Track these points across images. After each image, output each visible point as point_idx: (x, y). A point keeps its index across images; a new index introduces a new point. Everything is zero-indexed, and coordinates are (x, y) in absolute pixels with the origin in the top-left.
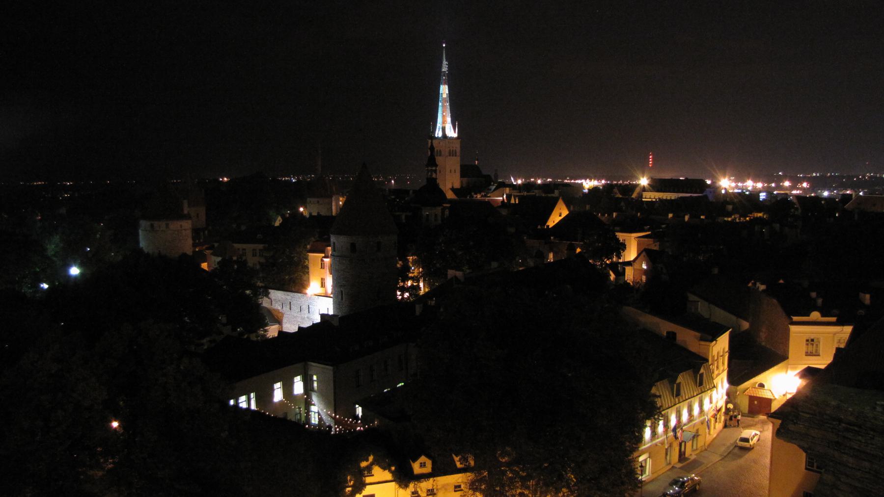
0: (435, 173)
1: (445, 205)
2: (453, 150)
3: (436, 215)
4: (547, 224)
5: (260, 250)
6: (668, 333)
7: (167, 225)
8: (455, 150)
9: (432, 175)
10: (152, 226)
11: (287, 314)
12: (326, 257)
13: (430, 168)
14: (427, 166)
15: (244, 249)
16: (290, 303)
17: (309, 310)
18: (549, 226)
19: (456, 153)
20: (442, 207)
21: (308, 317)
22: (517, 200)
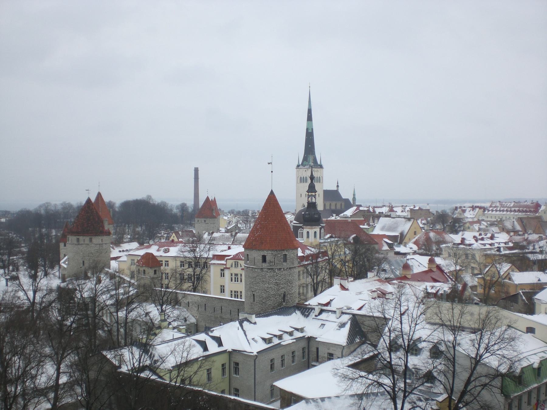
0: (315, 197)
1: (322, 225)
3: (315, 232)
4: (404, 241)
5: (166, 261)
6: (527, 328)
7: (91, 240)
8: (319, 177)
9: (312, 199)
10: (78, 240)
11: (202, 314)
12: (226, 268)
13: (310, 194)
14: (308, 192)
16: (205, 304)
20: (321, 227)
21: (221, 317)
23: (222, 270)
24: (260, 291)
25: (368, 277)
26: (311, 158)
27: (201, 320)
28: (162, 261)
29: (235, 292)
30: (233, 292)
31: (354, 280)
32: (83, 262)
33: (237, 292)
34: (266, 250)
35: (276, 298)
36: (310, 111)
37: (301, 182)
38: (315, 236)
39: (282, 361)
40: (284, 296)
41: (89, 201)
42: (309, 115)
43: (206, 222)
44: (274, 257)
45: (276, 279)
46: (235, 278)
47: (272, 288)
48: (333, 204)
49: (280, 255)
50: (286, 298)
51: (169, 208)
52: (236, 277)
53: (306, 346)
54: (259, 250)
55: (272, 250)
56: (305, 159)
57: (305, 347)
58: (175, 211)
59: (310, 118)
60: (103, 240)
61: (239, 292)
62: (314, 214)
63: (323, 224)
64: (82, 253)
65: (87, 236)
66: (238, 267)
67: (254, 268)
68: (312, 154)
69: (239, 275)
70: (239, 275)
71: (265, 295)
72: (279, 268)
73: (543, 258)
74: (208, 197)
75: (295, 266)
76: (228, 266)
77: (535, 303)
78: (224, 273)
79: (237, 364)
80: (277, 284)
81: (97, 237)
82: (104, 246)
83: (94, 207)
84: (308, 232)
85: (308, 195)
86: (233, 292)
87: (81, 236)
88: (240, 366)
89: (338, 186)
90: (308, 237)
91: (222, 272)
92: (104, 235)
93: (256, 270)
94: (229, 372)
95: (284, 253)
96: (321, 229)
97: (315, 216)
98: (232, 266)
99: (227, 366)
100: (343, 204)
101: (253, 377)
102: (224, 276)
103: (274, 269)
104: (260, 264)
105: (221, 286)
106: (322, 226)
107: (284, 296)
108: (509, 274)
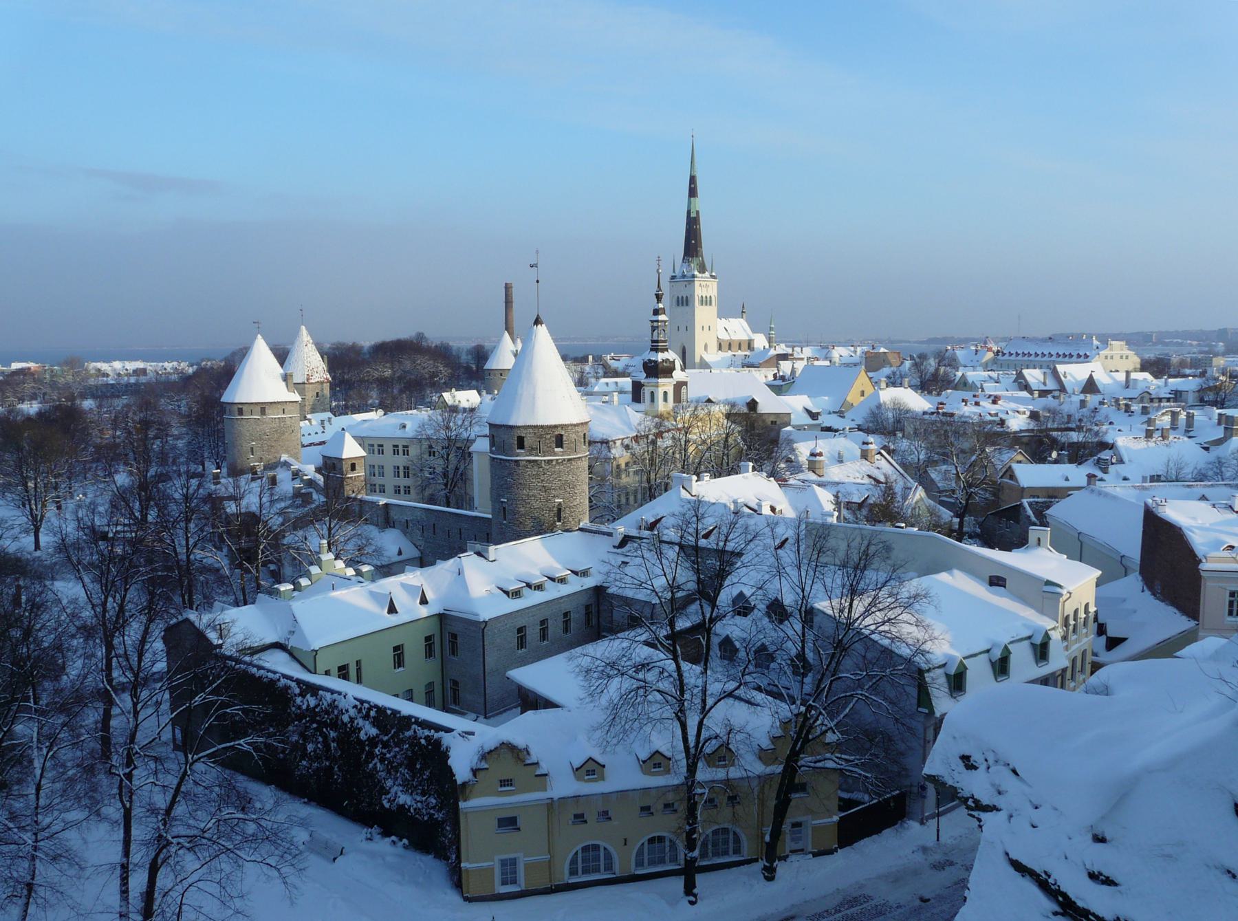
2: (706, 297)
3: (665, 393)
5: (404, 446)
6: (990, 577)
13: (655, 324)
15: (382, 446)
17: (461, 538)
19: (711, 301)
28: (397, 446)
36: (693, 180)
37: (678, 305)
38: (665, 399)
40: (559, 510)
42: (693, 186)
45: (542, 481)
47: (535, 497)
50: (563, 515)
51: (454, 353)
57: (591, 605)
58: (464, 358)
59: (693, 193)
67: (503, 460)
68: (697, 256)
72: (549, 460)
73: (1080, 440)
79: (454, 636)
80: (545, 489)
85: (652, 327)
88: (459, 640)
90: (652, 400)
94: (440, 651)
95: (557, 433)
99: (437, 640)
101: (482, 660)
107: (559, 510)
108: (1010, 467)
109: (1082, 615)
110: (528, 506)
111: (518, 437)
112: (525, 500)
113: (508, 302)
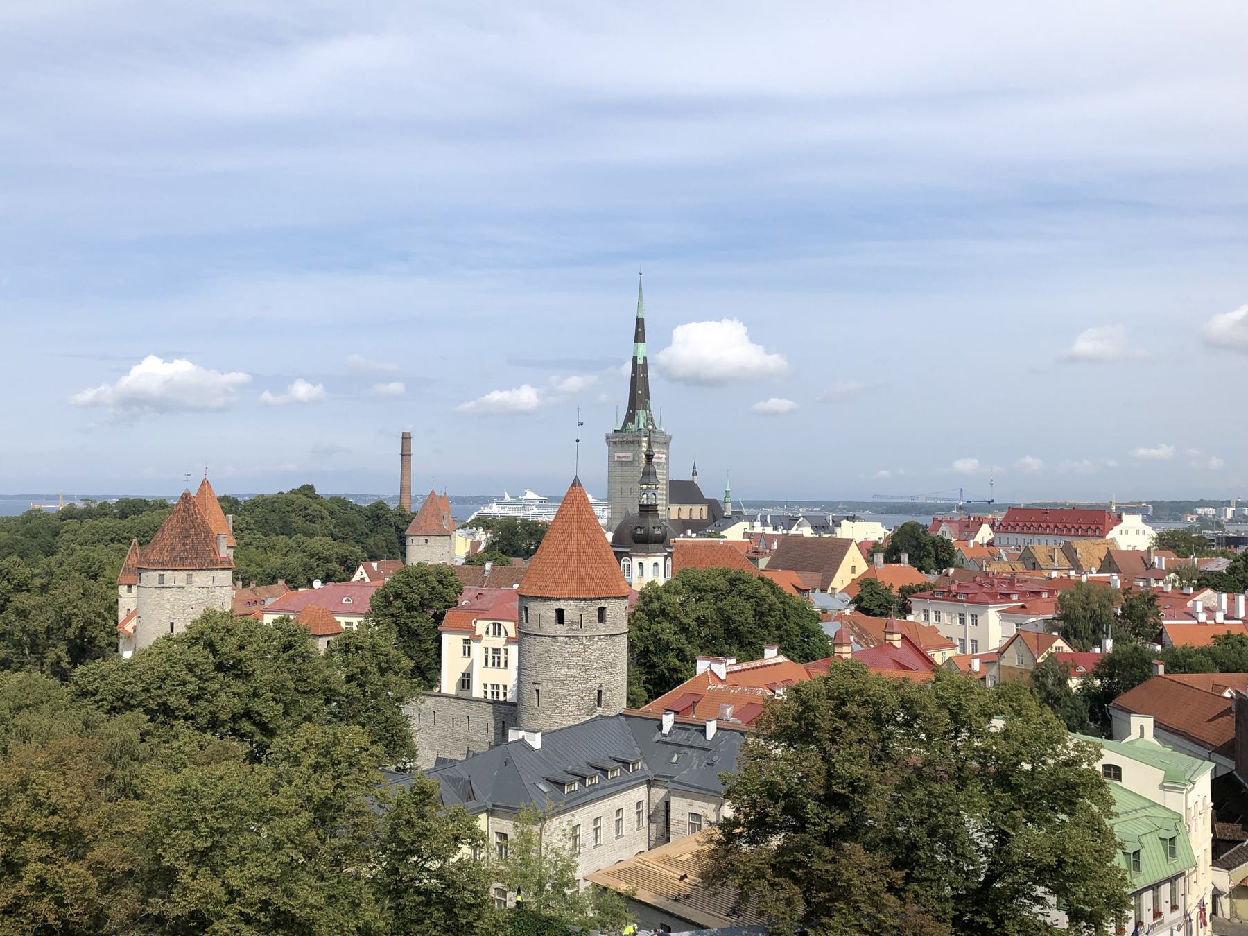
1: (669, 550)
3: (656, 564)
4: (832, 586)
5: (347, 623)
6: (1103, 766)
10: (162, 579)
18: (833, 589)
22: (775, 543)
23: (466, 641)
24: (550, 684)
25: (765, 657)
26: (641, 415)
27: (424, 745)
29: (493, 686)
30: (489, 687)
31: (738, 661)
32: (172, 624)
33: (498, 686)
34: (564, 599)
35: (582, 698)
36: (640, 322)
38: (656, 574)
39: (596, 829)
40: (600, 692)
41: (186, 498)
43: (429, 544)
44: (580, 613)
45: (583, 659)
46: (494, 657)
47: (574, 677)
48: (686, 508)
49: (592, 609)
52: (496, 656)
53: (644, 798)
54: (550, 599)
55: (577, 599)
56: (630, 418)
59: (640, 337)
60: (216, 578)
61: (501, 688)
62: (654, 528)
63: (671, 548)
64: (169, 607)
65: (181, 570)
66: (499, 634)
69: (502, 652)
70: (502, 652)
71: (560, 691)
74: (433, 492)
75: (622, 631)
76: (477, 633)
77: (1111, 716)
78: (469, 648)
80: (586, 669)
81: (203, 572)
82: (218, 591)
83: (199, 510)
84: (641, 564)
86: (489, 687)
87: (169, 570)
89: (694, 474)
91: (467, 646)
92: (217, 569)
93: (543, 639)
95: (600, 606)
96: (666, 557)
97: (656, 532)
98: (487, 633)
100: (705, 508)
102: (469, 654)
103: (580, 638)
104: (552, 627)
105: (464, 674)
106: (669, 552)
109: (1200, 808)
110: (566, 687)
111: (557, 610)
112: (562, 681)
113: (406, 454)
